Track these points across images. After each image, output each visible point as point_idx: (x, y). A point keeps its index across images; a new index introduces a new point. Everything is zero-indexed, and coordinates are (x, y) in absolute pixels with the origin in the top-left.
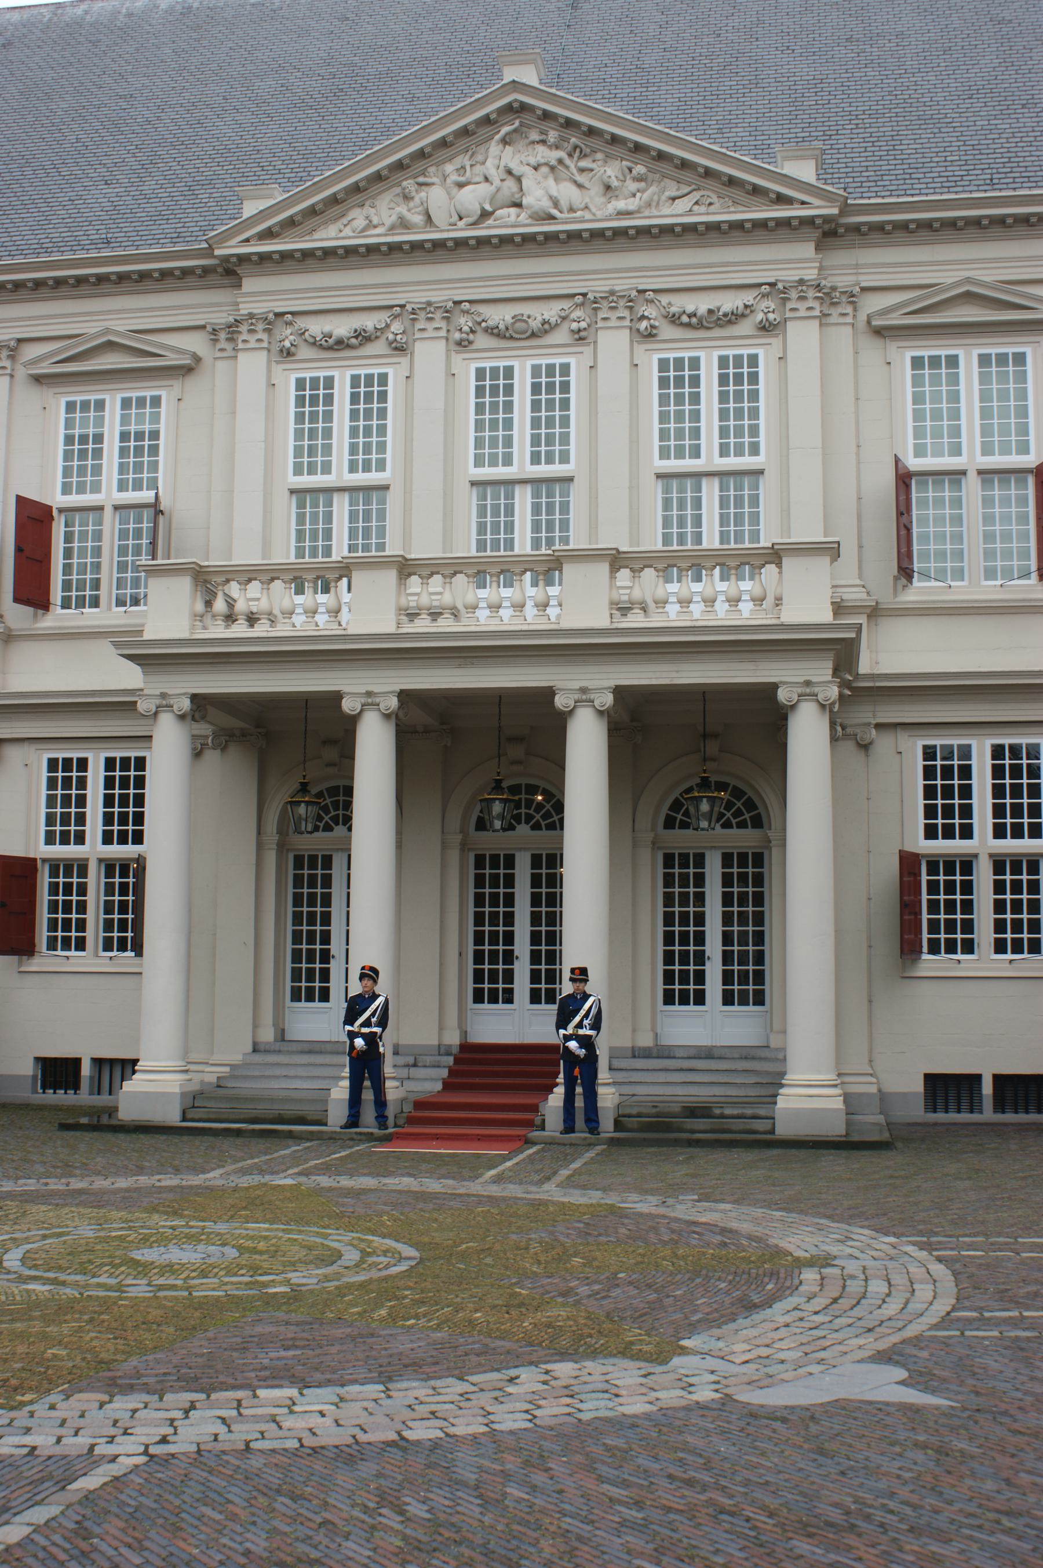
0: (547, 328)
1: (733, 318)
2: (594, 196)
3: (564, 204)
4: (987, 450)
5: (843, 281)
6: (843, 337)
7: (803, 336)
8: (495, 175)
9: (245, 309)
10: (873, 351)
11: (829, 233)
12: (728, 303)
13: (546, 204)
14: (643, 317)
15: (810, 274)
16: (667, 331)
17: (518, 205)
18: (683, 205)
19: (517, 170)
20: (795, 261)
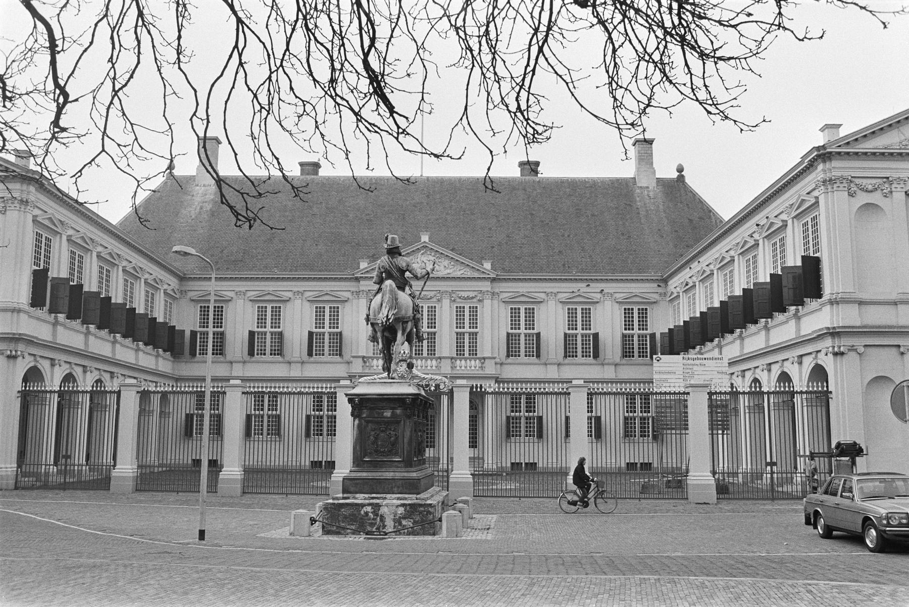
0: (431, 298)
1: (473, 298)
2: (442, 268)
5: (497, 290)
6: (495, 302)
7: (487, 302)
9: (361, 289)
10: (502, 305)
11: (493, 280)
12: (472, 294)
15: (489, 289)
16: (458, 300)
18: (462, 272)
20: (486, 286)
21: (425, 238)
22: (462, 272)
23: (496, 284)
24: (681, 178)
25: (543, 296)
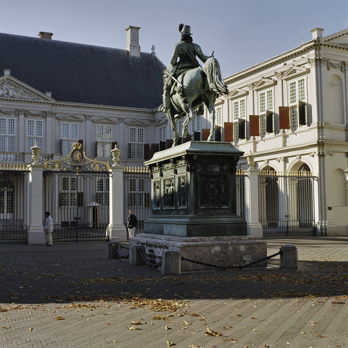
1: (39, 115)
3: (15, 95)
4: (72, 137)
5: (54, 111)
6: (54, 119)
8: (5, 89)
11: (53, 104)
13: (13, 95)
14: (26, 114)
15: (50, 110)
16: (29, 116)
17: (8, 94)
18: (32, 98)
19: (8, 89)
21: (7, 73)
22: (32, 98)
23: (54, 108)
24: (153, 53)
25: (83, 117)
